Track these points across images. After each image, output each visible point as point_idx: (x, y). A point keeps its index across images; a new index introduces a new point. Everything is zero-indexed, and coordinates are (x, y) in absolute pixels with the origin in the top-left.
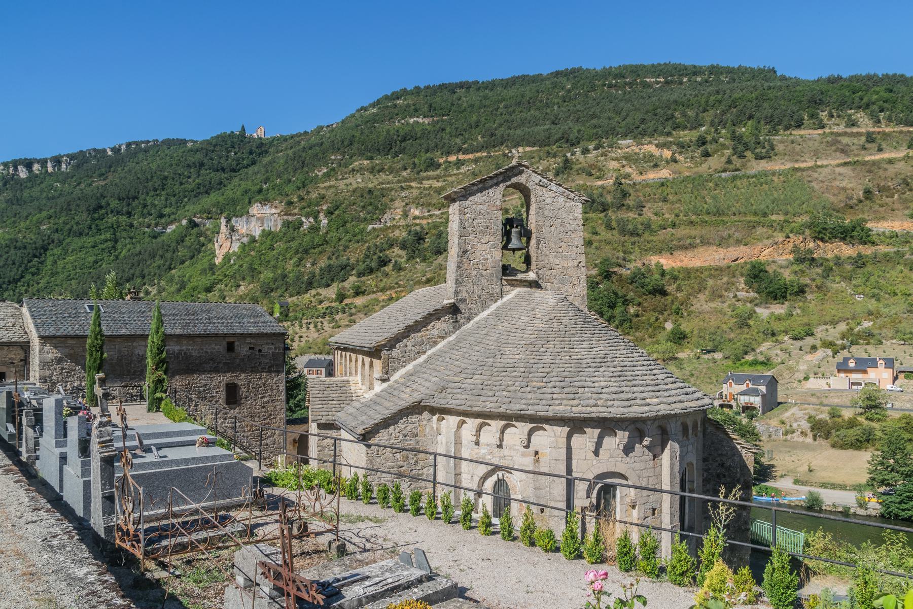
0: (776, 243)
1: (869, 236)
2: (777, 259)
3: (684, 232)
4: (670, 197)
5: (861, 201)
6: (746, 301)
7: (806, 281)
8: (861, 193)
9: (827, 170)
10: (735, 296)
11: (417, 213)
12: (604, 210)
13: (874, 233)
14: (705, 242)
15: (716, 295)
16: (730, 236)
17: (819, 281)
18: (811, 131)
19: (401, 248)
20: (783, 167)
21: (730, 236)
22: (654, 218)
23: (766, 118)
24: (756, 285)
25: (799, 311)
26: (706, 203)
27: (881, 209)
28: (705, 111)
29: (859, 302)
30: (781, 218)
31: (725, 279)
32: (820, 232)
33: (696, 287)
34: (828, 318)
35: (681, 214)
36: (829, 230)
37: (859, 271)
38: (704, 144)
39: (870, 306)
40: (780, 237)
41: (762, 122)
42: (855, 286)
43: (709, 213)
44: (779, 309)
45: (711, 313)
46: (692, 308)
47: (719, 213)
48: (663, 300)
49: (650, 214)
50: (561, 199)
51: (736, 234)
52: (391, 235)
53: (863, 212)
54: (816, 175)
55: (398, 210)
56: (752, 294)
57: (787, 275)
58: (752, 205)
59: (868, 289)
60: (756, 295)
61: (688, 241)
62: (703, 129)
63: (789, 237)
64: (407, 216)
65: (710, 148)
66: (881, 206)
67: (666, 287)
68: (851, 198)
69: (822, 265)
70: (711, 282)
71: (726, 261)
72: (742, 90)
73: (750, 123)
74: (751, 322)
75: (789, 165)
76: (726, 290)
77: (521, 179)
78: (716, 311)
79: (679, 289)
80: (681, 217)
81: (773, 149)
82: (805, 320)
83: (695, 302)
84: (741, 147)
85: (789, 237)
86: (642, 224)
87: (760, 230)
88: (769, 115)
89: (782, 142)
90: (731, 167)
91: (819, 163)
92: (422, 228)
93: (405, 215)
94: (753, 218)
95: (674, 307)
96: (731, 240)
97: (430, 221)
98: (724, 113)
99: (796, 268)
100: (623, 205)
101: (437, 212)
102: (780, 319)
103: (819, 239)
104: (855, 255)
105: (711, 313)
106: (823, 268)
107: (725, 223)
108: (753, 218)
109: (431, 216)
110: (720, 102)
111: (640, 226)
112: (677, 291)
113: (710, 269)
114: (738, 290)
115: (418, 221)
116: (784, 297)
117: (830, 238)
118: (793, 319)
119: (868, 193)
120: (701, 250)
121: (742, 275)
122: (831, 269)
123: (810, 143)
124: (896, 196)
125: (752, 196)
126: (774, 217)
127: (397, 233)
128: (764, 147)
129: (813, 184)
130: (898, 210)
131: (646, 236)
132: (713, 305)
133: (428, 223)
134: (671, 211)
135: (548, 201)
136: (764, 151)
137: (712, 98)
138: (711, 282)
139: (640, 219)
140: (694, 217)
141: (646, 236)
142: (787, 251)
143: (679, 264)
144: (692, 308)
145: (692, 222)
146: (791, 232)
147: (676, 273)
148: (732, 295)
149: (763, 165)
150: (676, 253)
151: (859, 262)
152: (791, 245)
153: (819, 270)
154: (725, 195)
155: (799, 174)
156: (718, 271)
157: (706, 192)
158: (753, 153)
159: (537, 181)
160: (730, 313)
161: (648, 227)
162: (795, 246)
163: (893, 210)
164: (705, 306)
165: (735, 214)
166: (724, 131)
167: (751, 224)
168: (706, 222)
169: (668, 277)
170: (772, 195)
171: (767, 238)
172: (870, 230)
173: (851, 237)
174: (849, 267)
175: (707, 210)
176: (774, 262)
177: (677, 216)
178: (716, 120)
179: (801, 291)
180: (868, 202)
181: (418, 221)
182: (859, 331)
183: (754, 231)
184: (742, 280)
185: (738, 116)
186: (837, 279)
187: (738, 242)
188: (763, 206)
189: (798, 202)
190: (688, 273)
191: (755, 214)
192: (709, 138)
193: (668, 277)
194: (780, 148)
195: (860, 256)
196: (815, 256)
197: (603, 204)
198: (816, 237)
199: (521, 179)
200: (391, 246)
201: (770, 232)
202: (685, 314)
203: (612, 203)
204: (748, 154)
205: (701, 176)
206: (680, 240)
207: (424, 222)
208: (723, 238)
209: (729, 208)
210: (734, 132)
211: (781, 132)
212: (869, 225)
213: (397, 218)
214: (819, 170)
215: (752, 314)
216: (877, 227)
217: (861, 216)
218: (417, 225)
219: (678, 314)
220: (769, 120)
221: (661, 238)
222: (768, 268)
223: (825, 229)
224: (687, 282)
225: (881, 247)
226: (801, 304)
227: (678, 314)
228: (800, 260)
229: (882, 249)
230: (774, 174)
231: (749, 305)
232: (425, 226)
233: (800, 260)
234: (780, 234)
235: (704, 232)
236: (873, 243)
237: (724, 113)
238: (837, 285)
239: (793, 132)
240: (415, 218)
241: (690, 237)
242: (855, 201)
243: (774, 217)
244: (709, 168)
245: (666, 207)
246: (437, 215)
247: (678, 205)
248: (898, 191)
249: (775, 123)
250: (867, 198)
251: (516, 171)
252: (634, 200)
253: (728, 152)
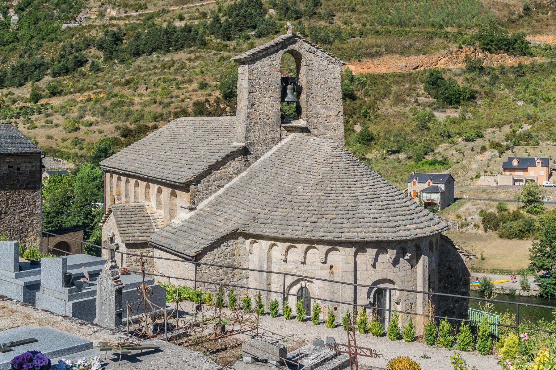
0: (451, 53)
1: (528, 48)
2: (452, 67)
3: (370, 41)
4: (358, 7)
5: (521, 17)
6: (425, 105)
7: (476, 88)
8: (521, 9)
10: (416, 101)
11: (114, 13)
12: (298, 18)
13: (532, 45)
14: (390, 51)
15: (399, 100)
16: (411, 46)
17: (487, 88)
19: (98, 49)
21: (411, 46)
22: (343, 26)
24: (434, 91)
25: (470, 115)
26: (390, 14)
27: (537, 24)
29: (520, 107)
30: (455, 30)
31: (407, 85)
32: (487, 44)
33: (382, 92)
34: (495, 122)
35: (368, 24)
36: (495, 42)
37: (520, 79)
39: (529, 111)
40: (454, 48)
42: (517, 93)
43: (392, 24)
44: (454, 113)
45: (395, 116)
46: (379, 112)
47: (402, 24)
48: (352, 104)
49: (339, 23)
50: (325, 63)
51: (417, 44)
52: (87, 35)
53: (523, 27)
55: (94, 10)
56: (431, 100)
57: (460, 83)
58: (430, 17)
59: (527, 95)
60: (434, 100)
61: (375, 49)
63: (462, 48)
64: (104, 16)
66: (538, 21)
67: (355, 92)
68: (513, 14)
69: (489, 73)
70: (394, 88)
71: (408, 69)
74: (430, 125)
76: (408, 96)
77: (295, 47)
78: (399, 115)
79: (367, 94)
80: (368, 26)
82: (476, 123)
83: (381, 106)
85: (462, 48)
86: (333, 32)
87: (437, 41)
92: (120, 29)
93: (102, 15)
94: (431, 30)
95: (362, 111)
96: (412, 50)
97: (127, 22)
99: (467, 76)
100: (315, 13)
101: (135, 14)
102: (454, 123)
103: (486, 50)
104: (516, 65)
105: (395, 116)
106: (490, 76)
107: (407, 33)
108: (431, 30)
109: (128, 17)
111: (330, 34)
112: (365, 96)
113: (393, 75)
114: (418, 95)
115: (115, 22)
116: (458, 102)
117: (496, 50)
118: (465, 122)
119: (527, 9)
120: (386, 57)
121: (422, 82)
122: (497, 77)
124: (550, 13)
125: (429, 9)
126: (448, 29)
127: (93, 33)
130: (551, 25)
131: (337, 42)
132: (397, 109)
133: (126, 25)
134: (358, 20)
135: (316, 64)
138: (394, 88)
139: (331, 27)
140: (379, 27)
141: (337, 42)
142: (460, 60)
143: (365, 71)
144: (379, 112)
145: (377, 32)
146: (464, 43)
147: (364, 79)
148: (413, 100)
150: (364, 60)
151: (520, 71)
152: (463, 55)
153: (487, 78)
154: (406, 7)
156: (400, 78)
157: (389, 4)
159: (307, 49)
160: (412, 117)
161: (338, 35)
162: (467, 56)
163: (547, 26)
164: (390, 110)
165: (415, 26)
167: (429, 35)
168: (390, 32)
169: (357, 83)
170: (447, 8)
171: (444, 48)
172: (529, 43)
173: (514, 49)
174: (511, 76)
175: (391, 20)
176: (449, 70)
177: (364, 25)
179: (472, 97)
180: (527, 18)
181: (115, 22)
182: (520, 134)
183: (432, 41)
184: (422, 86)
186: (502, 86)
187: (419, 51)
188: (438, 20)
189: (469, 16)
190: (375, 79)
191: (433, 25)
193: (357, 83)
195: (520, 66)
196: (484, 65)
197: (296, 12)
198: (484, 48)
199: (295, 47)
200: (88, 46)
201: (446, 43)
202: (372, 117)
203: (305, 11)
206: (367, 48)
207: (121, 23)
208: (405, 47)
209: (410, 19)
212: (528, 38)
213: (93, 17)
215: (431, 118)
216: (535, 40)
217: (521, 30)
218: (114, 25)
219: (366, 117)
221: (351, 46)
222: (444, 76)
223: (492, 41)
224: (374, 88)
225: (537, 58)
226: (472, 108)
227: (366, 117)
228: (471, 69)
229: (539, 60)
231: (428, 109)
232: (122, 27)
233: (471, 69)
234: (454, 45)
235: (388, 41)
236: (531, 55)
238: (502, 91)
240: (112, 18)
241: (376, 46)
242: (516, 16)
243: (448, 29)
245: (354, 16)
246: (134, 17)
247: (365, 15)
248: (551, 9)
250: (526, 14)
251: (291, 41)
252: (325, 9)
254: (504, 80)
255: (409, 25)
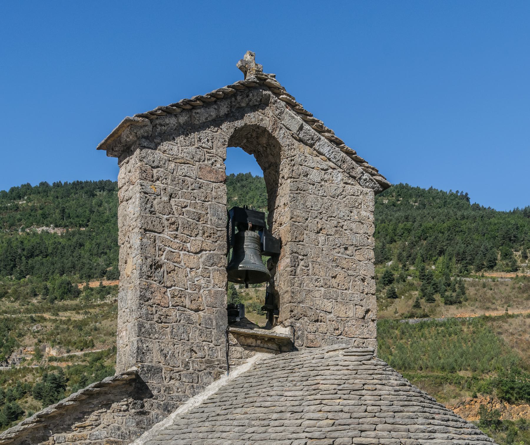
9: (518, 321)
18: (503, 274)
20: (473, 316)
23: (458, 254)
26: (391, 354)
28: (392, 241)
30: (469, 374)
32: (507, 392)
36: (517, 390)
38: (390, 282)
40: (467, 396)
41: (454, 259)
54: (506, 326)
58: (440, 358)
62: (390, 263)
63: (476, 397)
65: (397, 287)
69: (507, 429)
72: (433, 218)
73: (441, 259)
75: (479, 313)
81: (464, 293)
84: (431, 288)
85: (476, 397)
87: (447, 388)
88: (462, 250)
89: (473, 285)
90: (419, 312)
91: (510, 312)
94: (440, 374)
98: (413, 245)
103: (505, 400)
106: (508, 432)
108: (440, 374)
110: (409, 231)
117: (516, 399)
122: (516, 434)
123: (502, 288)
125: (440, 348)
126: (461, 374)
128: (454, 290)
129: (503, 337)
136: (454, 294)
137: (401, 225)
142: (474, 412)
146: (479, 391)
149: (454, 312)
152: (478, 406)
153: (504, 435)
154: (411, 345)
155: (489, 324)
157: (391, 341)
158: (442, 296)
162: (482, 407)
165: (421, 369)
166: (412, 268)
167: (438, 380)
170: (461, 347)
171: (455, 397)
175: (393, 362)
178: (405, 254)
183: (441, 388)
185: (428, 250)
189: (487, 356)
191: (443, 369)
192: (396, 275)
194: (471, 292)
196: (501, 419)
198: (503, 398)
201: (457, 390)
204: (437, 297)
205: (386, 321)
209: (416, 360)
210: (423, 269)
211: (473, 273)
214: (510, 320)
220: (461, 257)
230: (463, 322)
233: (486, 423)
234: (467, 393)
237: (413, 245)
239: (486, 274)
243: (461, 374)
244: (396, 312)
249: (468, 261)
253: (416, 294)
254: (524, 436)
255: (414, 368)
